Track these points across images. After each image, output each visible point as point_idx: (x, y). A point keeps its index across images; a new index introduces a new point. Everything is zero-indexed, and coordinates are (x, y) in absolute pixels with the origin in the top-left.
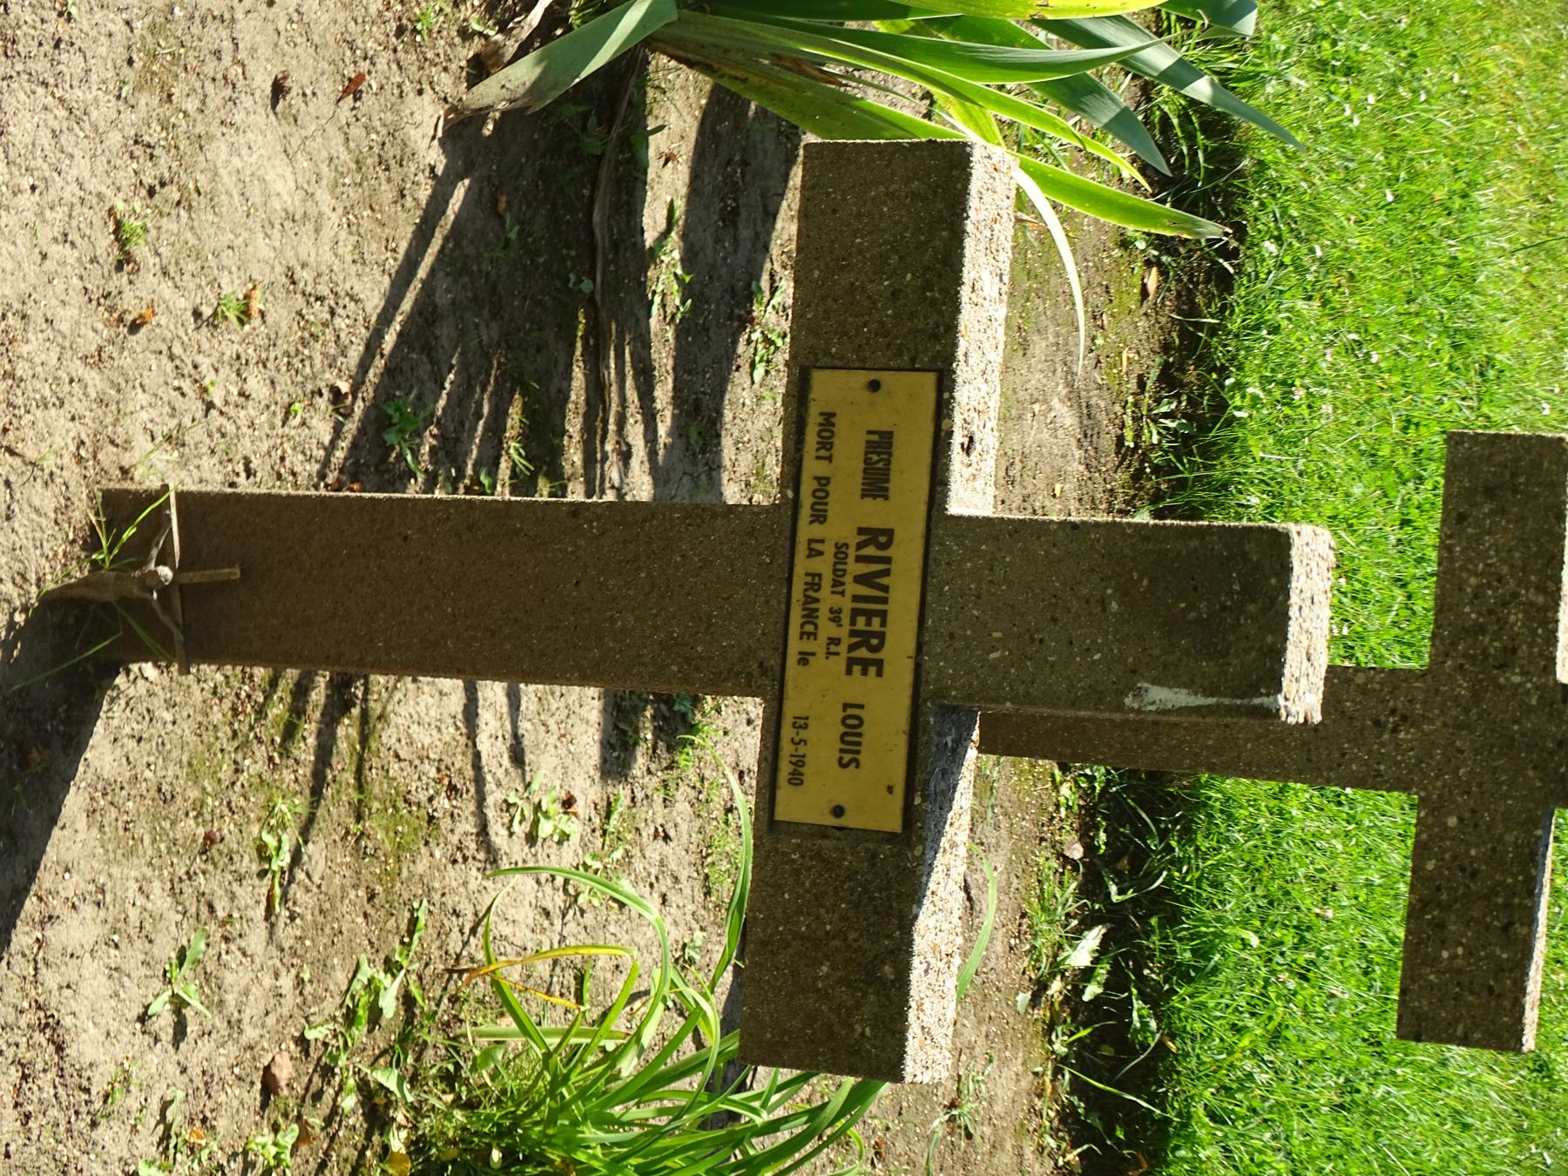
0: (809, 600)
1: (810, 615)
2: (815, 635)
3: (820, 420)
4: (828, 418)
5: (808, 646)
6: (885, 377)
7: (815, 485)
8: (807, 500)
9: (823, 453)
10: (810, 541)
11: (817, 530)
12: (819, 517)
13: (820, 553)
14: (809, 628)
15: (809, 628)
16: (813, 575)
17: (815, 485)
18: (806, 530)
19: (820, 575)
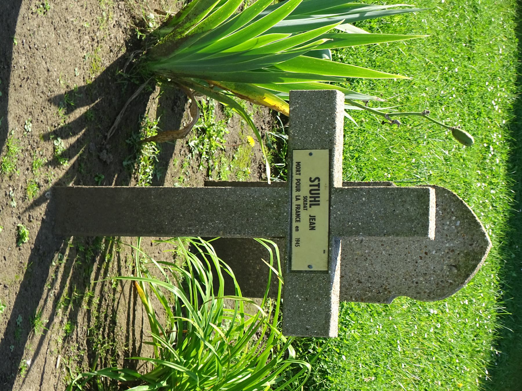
0: (297, 212)
1: (298, 216)
2: (300, 221)
3: (296, 164)
4: (298, 164)
5: (298, 224)
6: (312, 151)
7: (296, 181)
8: (294, 185)
9: (298, 173)
10: (296, 196)
11: (297, 193)
12: (298, 190)
13: (299, 199)
14: (298, 219)
15: (298, 219)
16: (298, 205)
17: (296, 181)
18: (295, 194)
19: (300, 205)
